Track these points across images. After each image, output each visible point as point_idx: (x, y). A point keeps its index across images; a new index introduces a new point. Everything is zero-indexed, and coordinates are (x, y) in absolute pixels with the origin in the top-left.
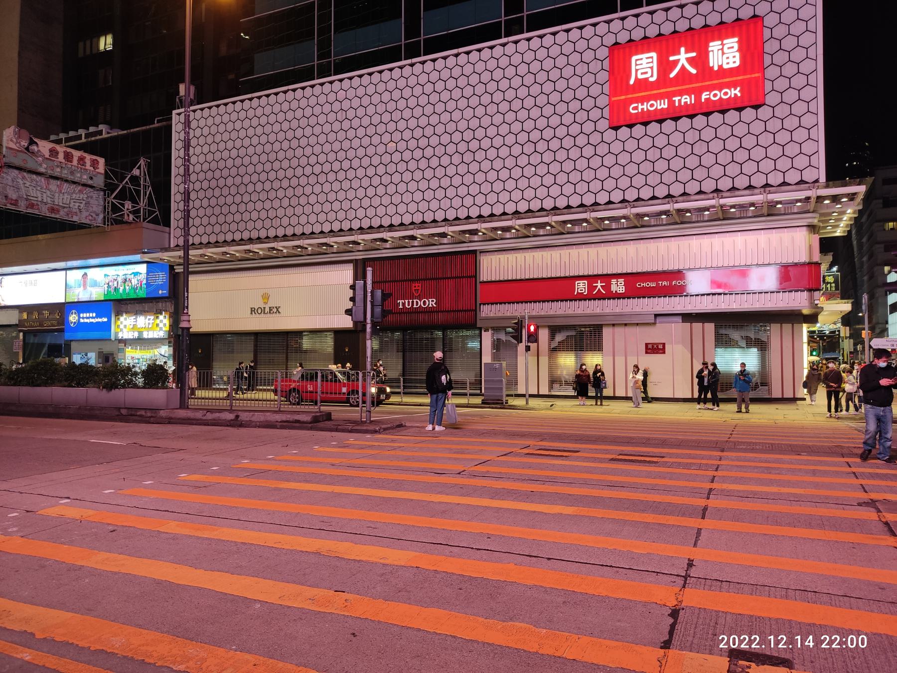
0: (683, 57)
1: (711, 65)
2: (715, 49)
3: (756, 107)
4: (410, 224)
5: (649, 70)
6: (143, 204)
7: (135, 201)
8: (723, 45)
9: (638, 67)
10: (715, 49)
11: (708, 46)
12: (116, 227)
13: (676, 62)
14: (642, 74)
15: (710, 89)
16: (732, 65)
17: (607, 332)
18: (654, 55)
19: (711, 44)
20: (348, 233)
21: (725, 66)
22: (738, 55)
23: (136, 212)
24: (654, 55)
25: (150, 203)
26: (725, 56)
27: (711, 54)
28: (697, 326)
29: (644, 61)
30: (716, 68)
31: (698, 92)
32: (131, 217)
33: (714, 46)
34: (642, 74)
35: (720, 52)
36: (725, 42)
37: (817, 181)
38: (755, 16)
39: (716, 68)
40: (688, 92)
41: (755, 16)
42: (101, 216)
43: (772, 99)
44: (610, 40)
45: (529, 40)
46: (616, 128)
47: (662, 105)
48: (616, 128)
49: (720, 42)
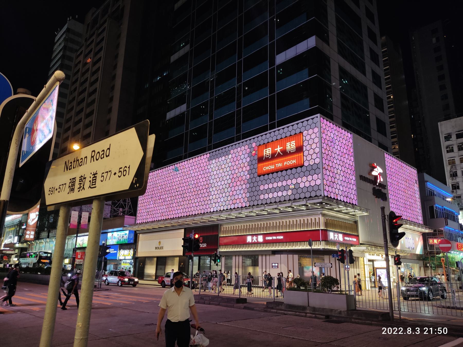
0: (278, 149)
2: (288, 145)
3: (302, 166)
4: (315, 196)
6: (126, 209)
7: (123, 208)
8: (291, 143)
11: (286, 144)
12: (116, 218)
15: (286, 161)
17: (260, 258)
18: (270, 148)
20: (249, 208)
23: (124, 212)
24: (270, 148)
25: (130, 208)
28: (290, 256)
29: (268, 151)
31: (283, 162)
32: (122, 214)
33: (288, 144)
37: (321, 195)
38: (300, 132)
40: (280, 162)
41: (300, 132)
42: (109, 214)
43: (306, 164)
44: (258, 144)
45: (270, 133)
46: (259, 176)
47: (272, 167)
48: (259, 176)
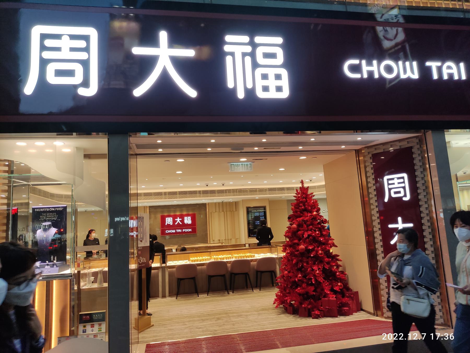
1: (230, 85)
2: (238, 50)
5: (79, 69)
9: (47, 55)
10: (238, 50)
13: (147, 64)
14: (59, 73)
16: (273, 95)
19: (229, 38)
21: (261, 94)
22: (284, 73)
26: (259, 71)
27: (229, 59)
30: (241, 95)
34: (59, 73)
35: (248, 60)
36: (258, 39)
39: (241, 95)
49: (246, 39)
